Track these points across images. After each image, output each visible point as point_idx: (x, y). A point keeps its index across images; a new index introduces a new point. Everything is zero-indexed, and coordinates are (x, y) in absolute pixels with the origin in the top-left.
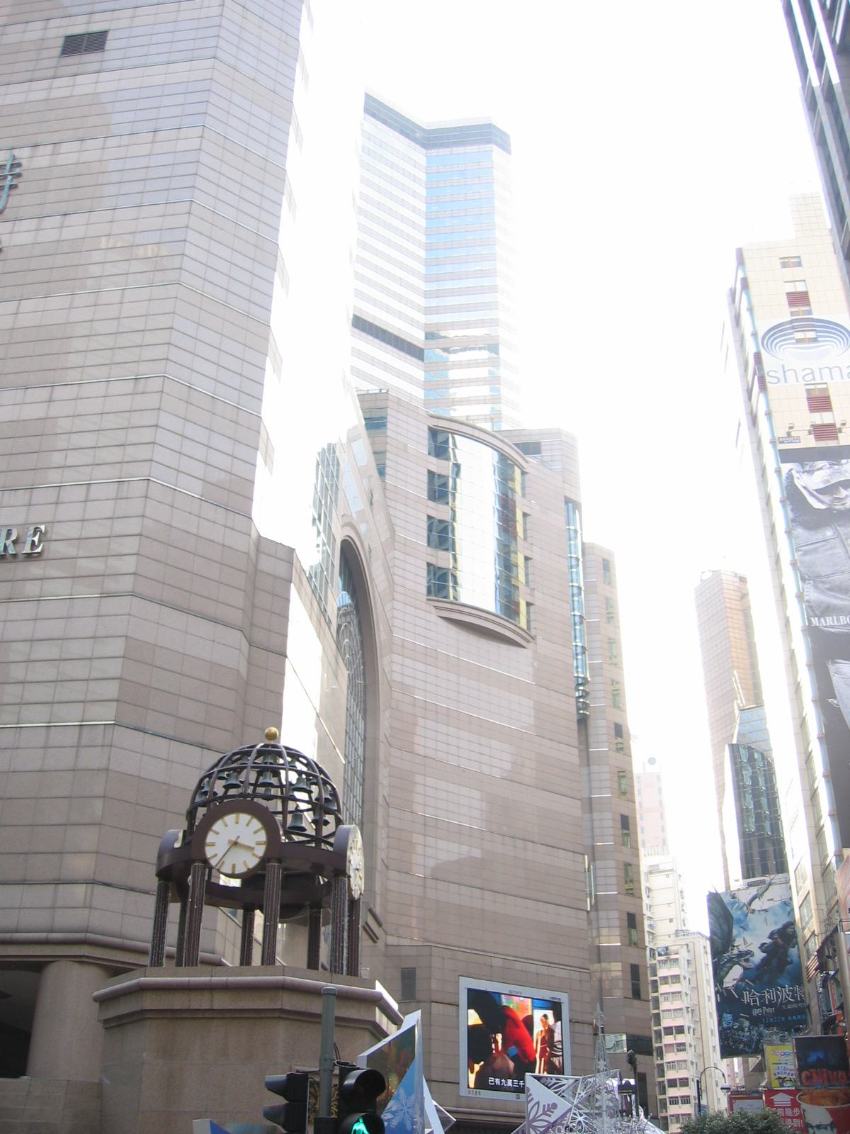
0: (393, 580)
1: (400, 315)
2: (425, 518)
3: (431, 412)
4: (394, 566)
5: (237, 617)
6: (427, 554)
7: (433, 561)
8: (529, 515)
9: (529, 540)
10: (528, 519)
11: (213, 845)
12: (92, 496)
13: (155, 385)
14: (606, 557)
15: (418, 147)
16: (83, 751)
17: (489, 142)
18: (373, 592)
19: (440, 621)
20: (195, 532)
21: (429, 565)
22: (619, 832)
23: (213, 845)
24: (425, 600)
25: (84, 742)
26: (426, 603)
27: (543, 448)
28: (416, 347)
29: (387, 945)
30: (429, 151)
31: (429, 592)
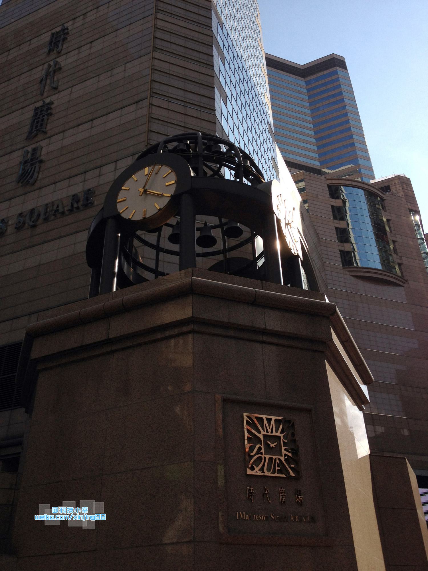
0: (323, 260)
2: (334, 228)
3: (327, 178)
4: (322, 254)
6: (339, 246)
7: (342, 248)
8: (391, 220)
10: (391, 222)
15: (300, 78)
17: (335, 66)
18: (312, 262)
19: (352, 278)
21: (340, 251)
24: (342, 268)
26: (343, 270)
30: (306, 79)
31: (343, 265)
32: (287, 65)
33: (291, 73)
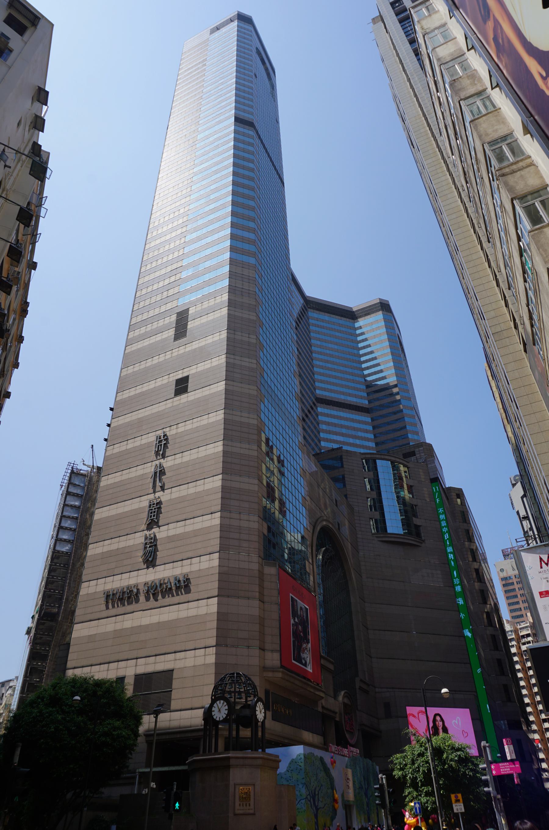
1: (356, 396)
9: (415, 497)
11: (214, 711)
12: (201, 561)
14: (458, 492)
16: (206, 656)
20: (237, 567)
23: (214, 711)
25: (206, 653)
27: (416, 453)
28: (365, 408)
32: (339, 308)
33: (342, 316)
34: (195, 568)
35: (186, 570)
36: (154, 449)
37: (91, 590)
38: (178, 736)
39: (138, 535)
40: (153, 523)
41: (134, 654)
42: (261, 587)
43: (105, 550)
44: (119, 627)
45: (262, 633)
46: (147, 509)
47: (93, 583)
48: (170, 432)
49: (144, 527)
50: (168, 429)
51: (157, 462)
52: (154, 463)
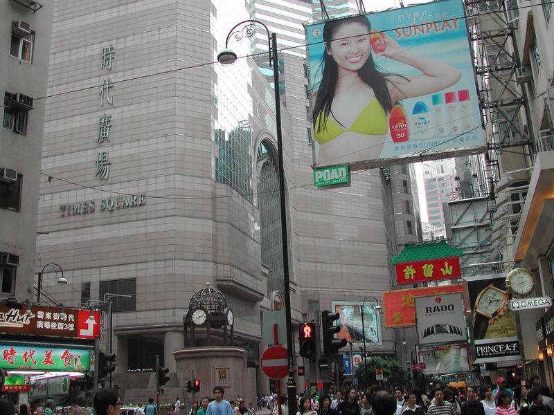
5: (210, 215)
13: (172, 138)
22: (407, 228)
29: (302, 292)
34: (152, 188)
35: (142, 190)
36: (99, 62)
37: (47, 204)
38: (145, 331)
39: (90, 152)
40: (103, 140)
41: (97, 263)
42: (214, 207)
43: (56, 166)
44: (79, 239)
45: (215, 248)
46: (98, 126)
47: (48, 197)
48: (119, 45)
49: (94, 145)
50: (114, 42)
51: (106, 78)
52: (102, 78)
